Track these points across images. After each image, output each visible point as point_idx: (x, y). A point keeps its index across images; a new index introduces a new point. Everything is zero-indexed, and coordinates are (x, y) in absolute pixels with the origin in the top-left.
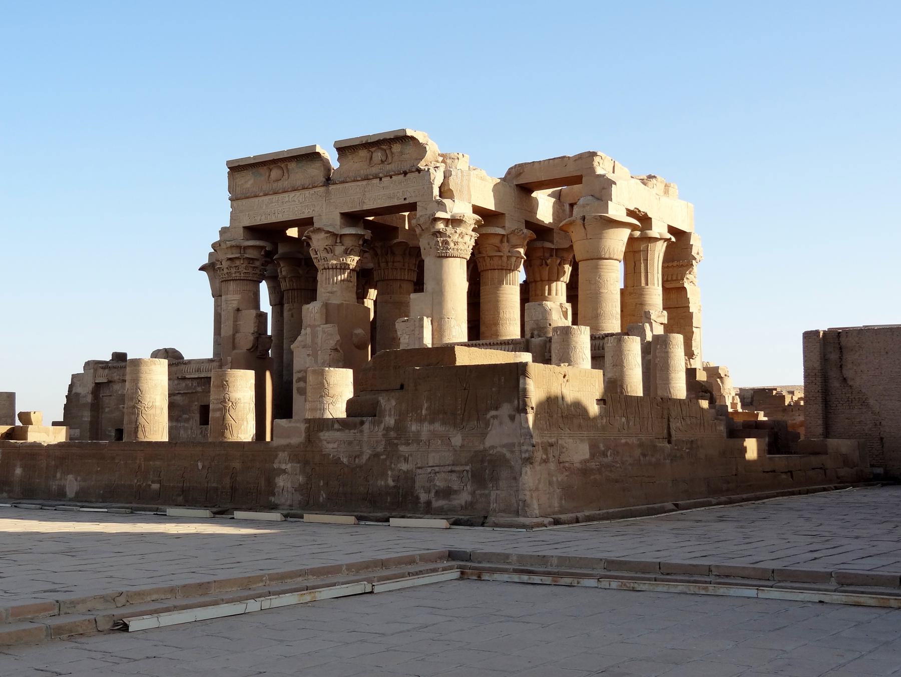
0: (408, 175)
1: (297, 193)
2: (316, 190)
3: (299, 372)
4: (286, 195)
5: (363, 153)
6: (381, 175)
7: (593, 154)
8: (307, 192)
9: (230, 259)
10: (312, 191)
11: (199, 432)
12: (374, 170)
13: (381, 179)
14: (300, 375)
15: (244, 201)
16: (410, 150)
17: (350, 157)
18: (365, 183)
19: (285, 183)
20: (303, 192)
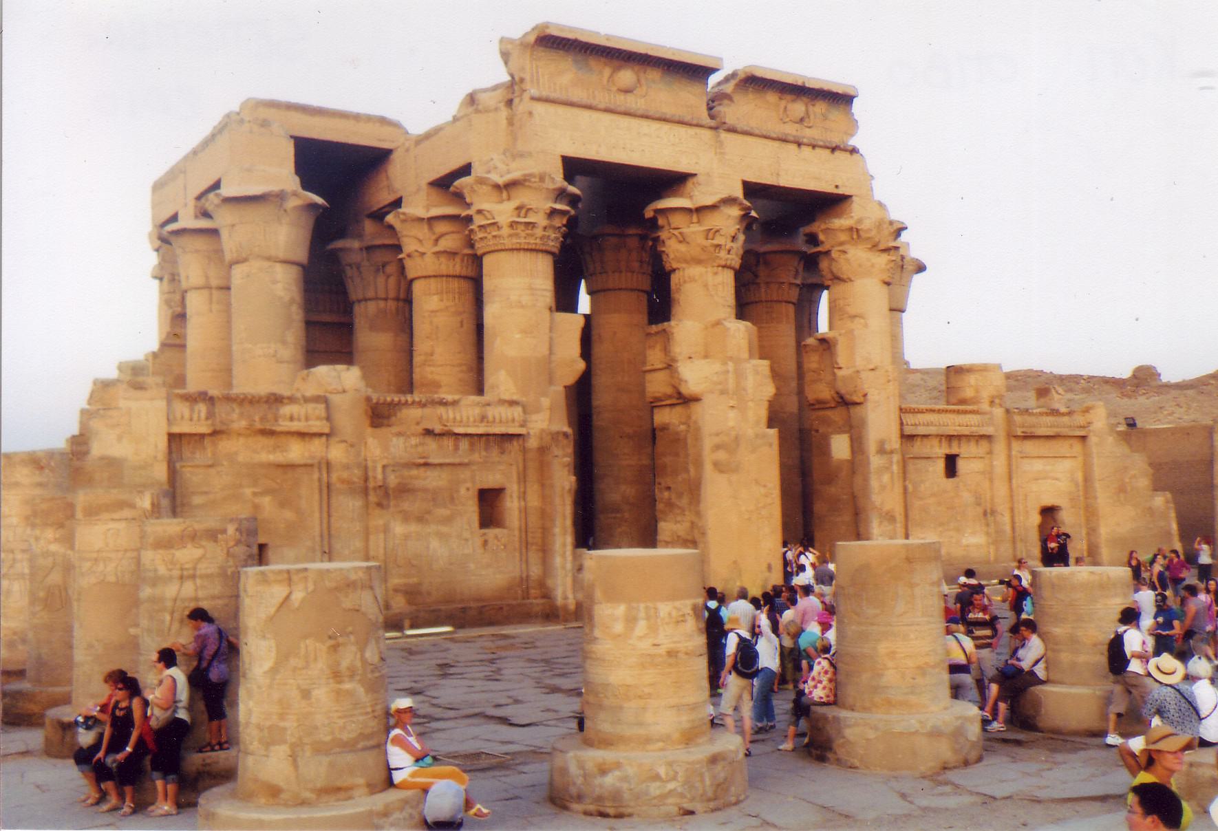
0: (837, 153)
2: (698, 130)
3: (717, 435)
5: (772, 97)
6: (805, 140)
9: (553, 213)
12: (791, 130)
14: (717, 440)
16: (836, 114)
17: (751, 96)
18: (776, 144)
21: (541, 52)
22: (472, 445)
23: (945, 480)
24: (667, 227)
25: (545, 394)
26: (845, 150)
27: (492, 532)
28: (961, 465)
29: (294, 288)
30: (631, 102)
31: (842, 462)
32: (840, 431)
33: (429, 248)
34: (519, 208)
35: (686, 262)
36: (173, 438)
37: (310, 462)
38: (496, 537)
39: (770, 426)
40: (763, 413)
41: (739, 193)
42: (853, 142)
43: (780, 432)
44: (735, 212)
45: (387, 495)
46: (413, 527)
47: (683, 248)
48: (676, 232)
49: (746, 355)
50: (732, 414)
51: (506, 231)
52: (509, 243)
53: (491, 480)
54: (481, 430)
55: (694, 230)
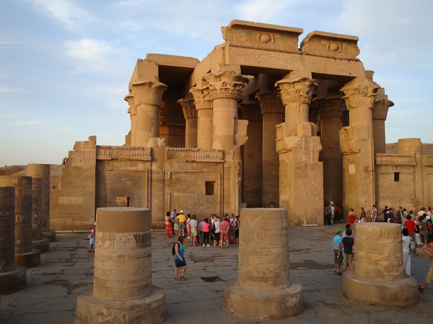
0: (351, 61)
1: (281, 54)
2: (294, 55)
4: (273, 53)
6: (338, 57)
7: (373, 72)
8: (288, 55)
10: (291, 55)
11: (205, 200)
12: (331, 54)
13: (335, 59)
15: (241, 49)
16: (351, 48)
17: (316, 42)
18: (326, 59)
19: (270, 46)
20: (284, 54)
21: (234, 30)
22: (203, 165)
23: (394, 182)
24: (283, 90)
25: (231, 149)
26: (354, 61)
27: (210, 196)
28: (401, 176)
29: (155, 113)
30: (268, 46)
31: (352, 175)
32: (352, 163)
33: (201, 99)
34: (223, 83)
35: (290, 101)
36: (98, 162)
37: (145, 170)
38: (211, 198)
39: (320, 160)
40: (317, 156)
41: (310, 77)
42: (358, 57)
43: (323, 163)
44: (307, 83)
45: (171, 182)
46: (181, 194)
47: (288, 97)
48: (286, 91)
49: (311, 135)
50: (304, 157)
51: (219, 92)
52: (220, 96)
53: (210, 179)
54: (207, 160)
55: (291, 90)
